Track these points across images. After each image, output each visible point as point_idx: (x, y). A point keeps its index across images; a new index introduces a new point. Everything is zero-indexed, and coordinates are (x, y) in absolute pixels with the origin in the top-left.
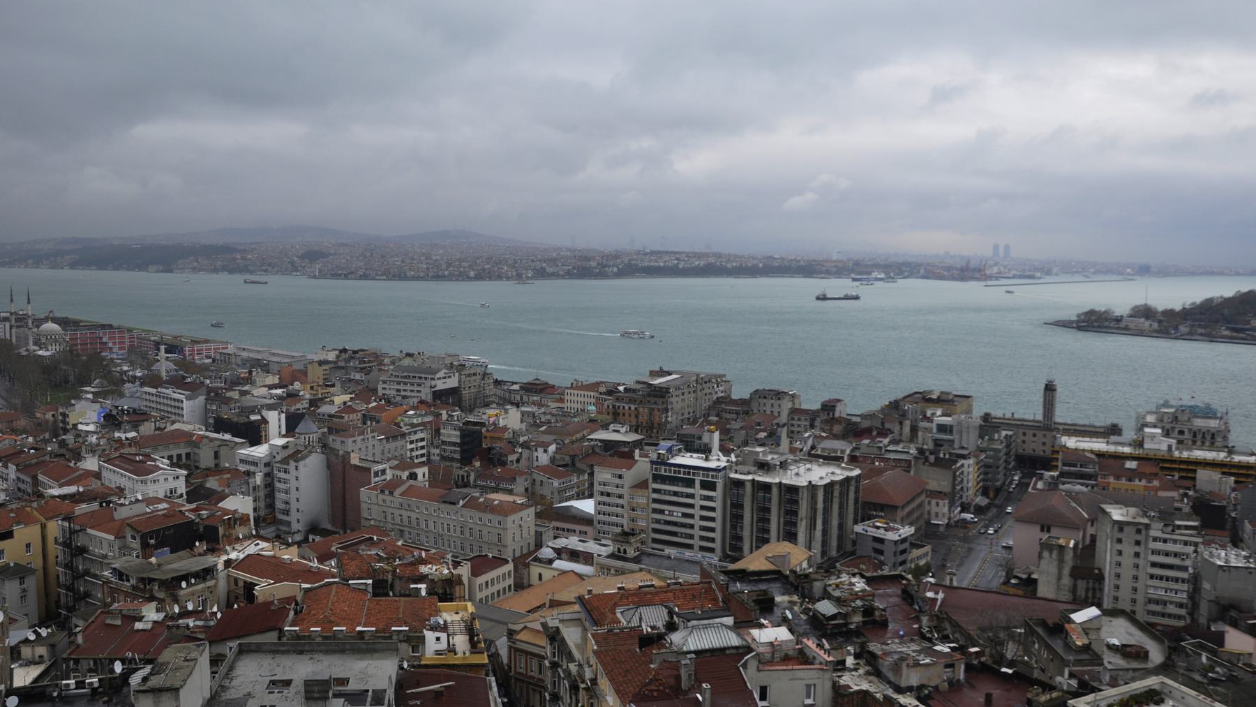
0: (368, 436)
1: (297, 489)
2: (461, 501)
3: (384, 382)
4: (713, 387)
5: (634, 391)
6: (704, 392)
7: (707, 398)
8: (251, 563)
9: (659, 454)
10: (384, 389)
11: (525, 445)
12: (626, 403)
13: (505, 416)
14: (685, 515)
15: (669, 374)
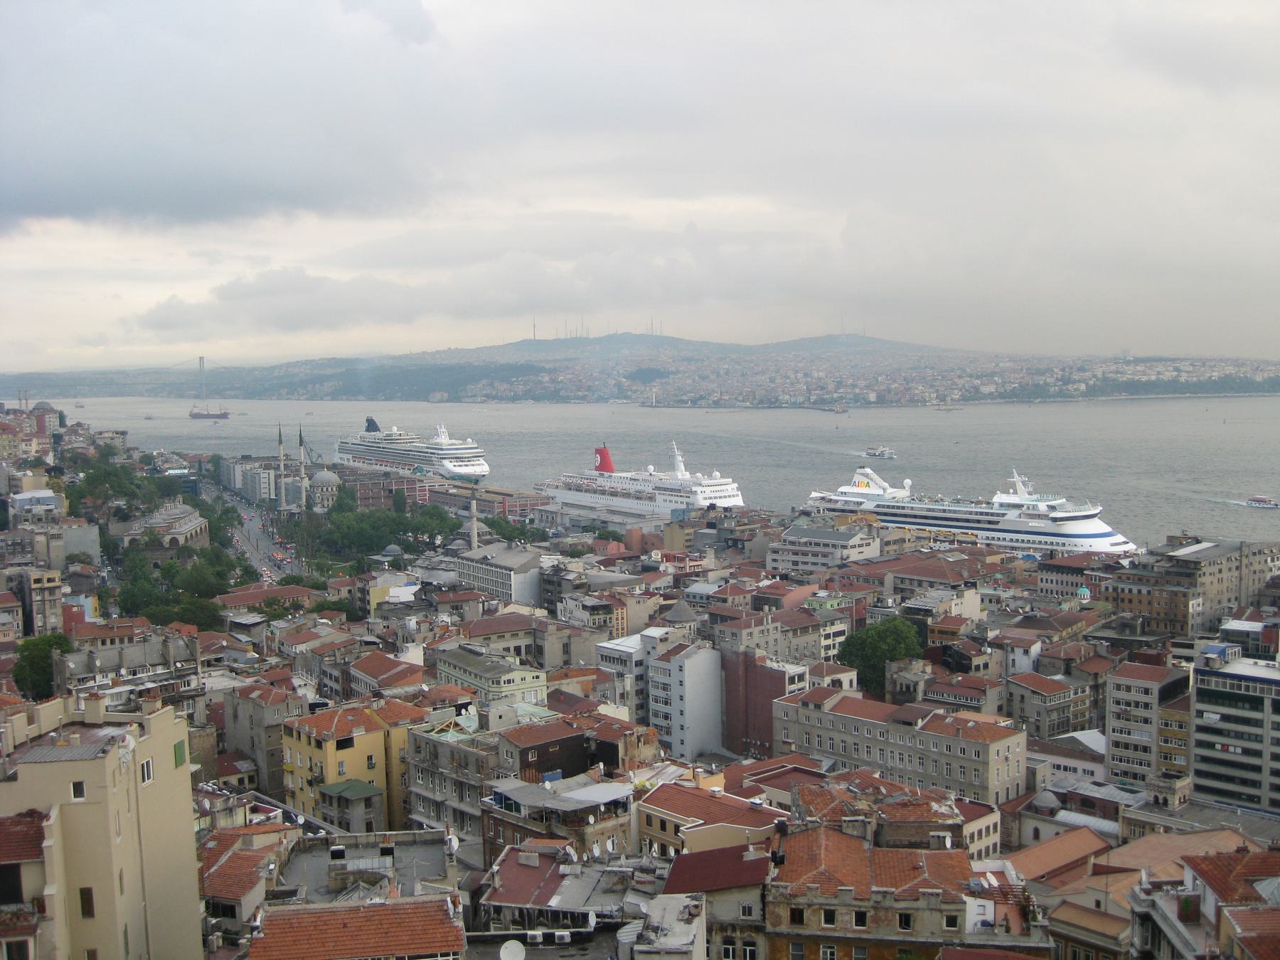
0: (768, 627)
1: (681, 698)
2: (920, 721)
3: (775, 551)
4: (1266, 561)
5: (1145, 566)
6: (1252, 568)
7: (1257, 577)
8: (668, 795)
9: (1208, 659)
10: (775, 560)
11: (996, 644)
12: (1134, 583)
13: (959, 601)
14: (1246, 752)
15: (1198, 541)
